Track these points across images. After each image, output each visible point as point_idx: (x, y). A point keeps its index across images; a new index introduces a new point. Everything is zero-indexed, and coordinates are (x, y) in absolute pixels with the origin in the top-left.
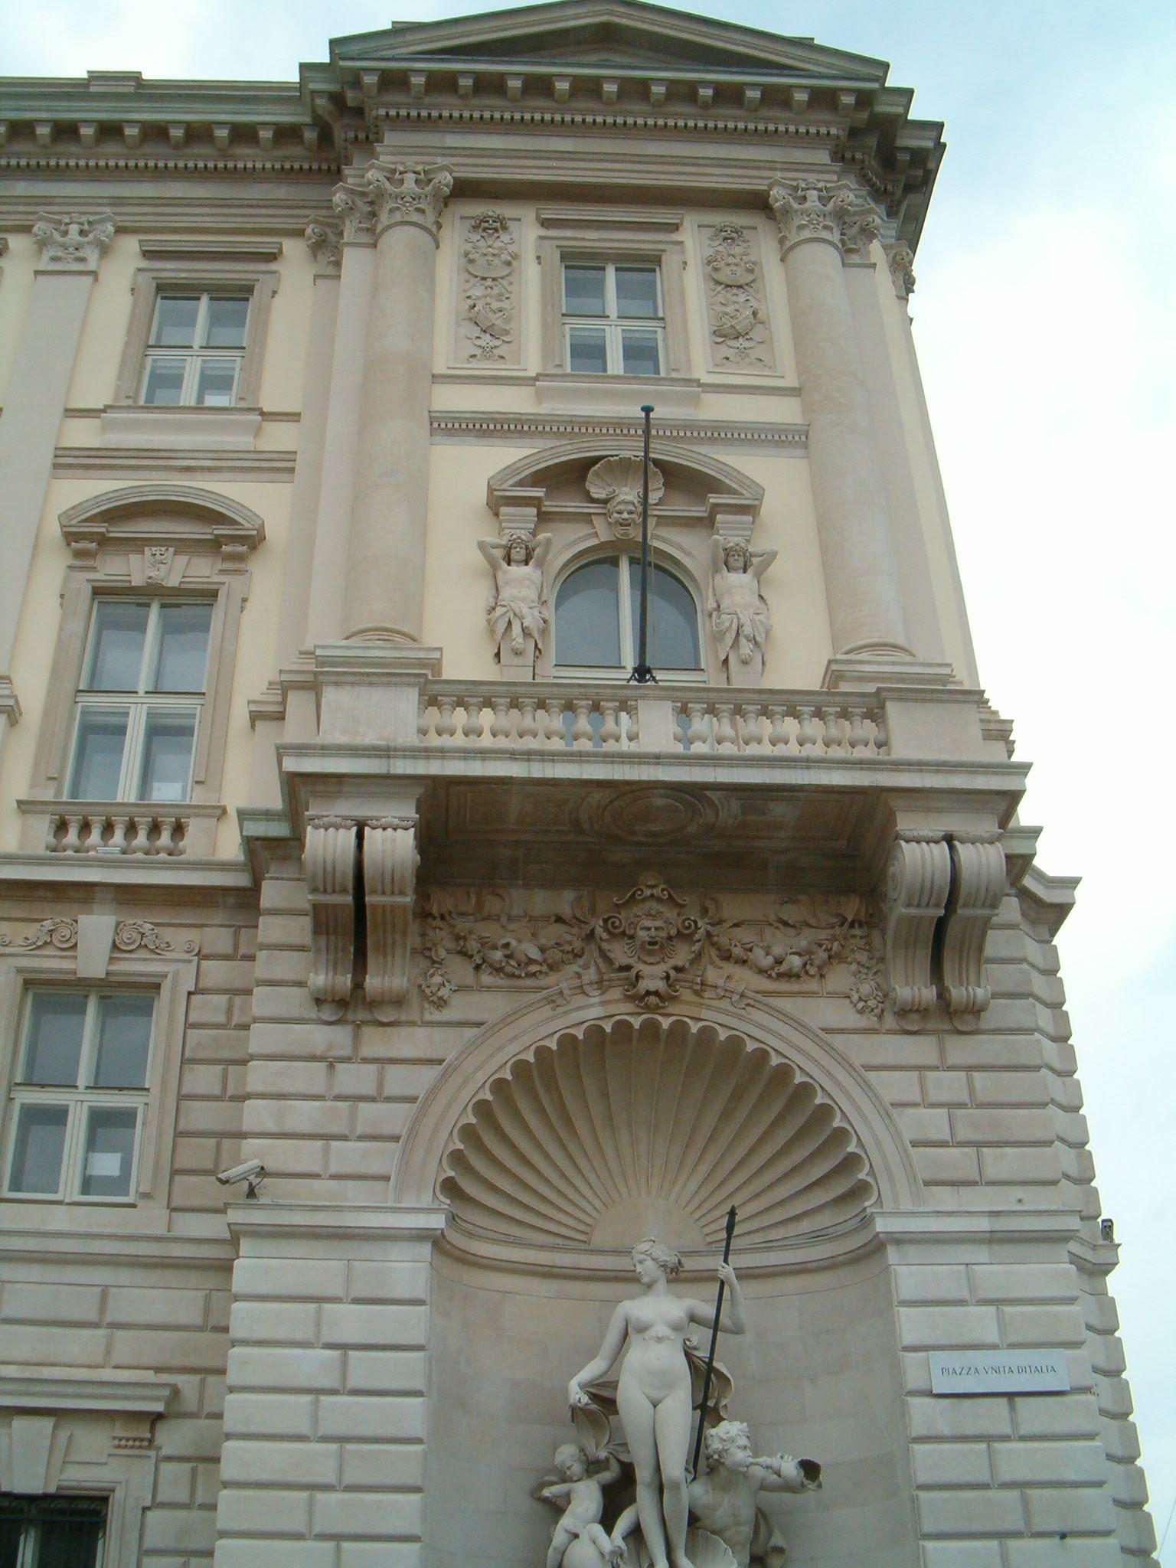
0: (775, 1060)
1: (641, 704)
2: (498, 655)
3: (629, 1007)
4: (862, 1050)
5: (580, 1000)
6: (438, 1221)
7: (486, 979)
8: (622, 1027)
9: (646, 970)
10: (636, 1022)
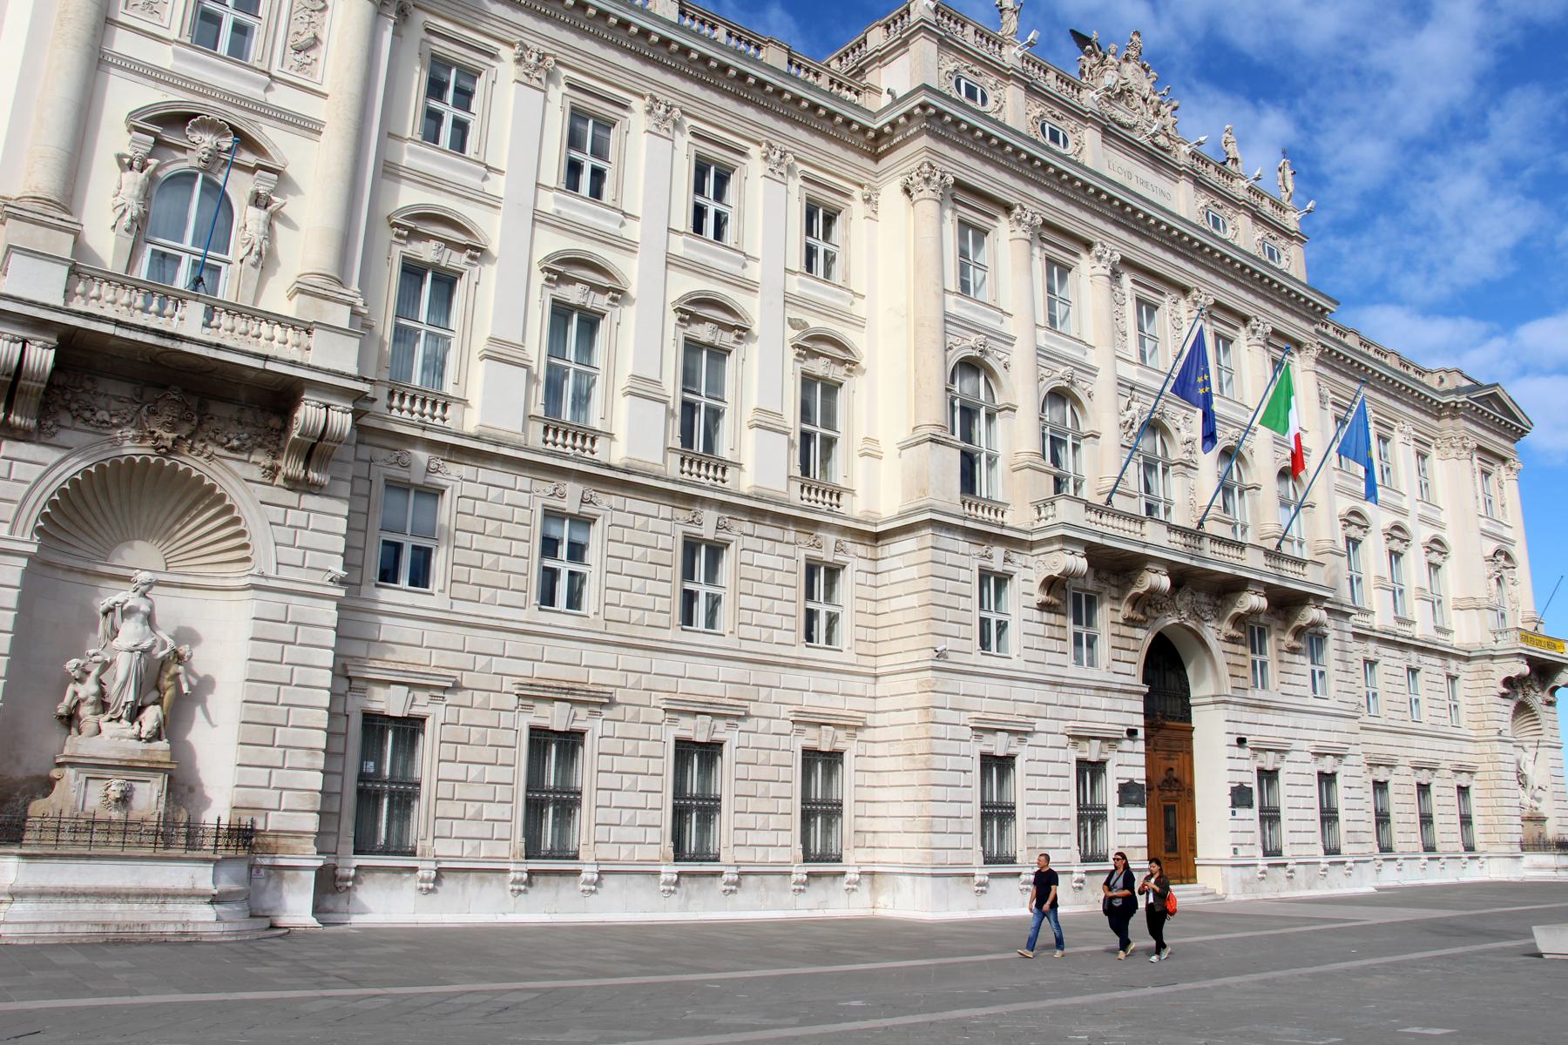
0: (218, 491)
1: (188, 302)
2: (114, 226)
3: (152, 452)
4: (264, 492)
5: (127, 443)
6: (34, 549)
7: (79, 424)
8: (145, 461)
9: (165, 435)
10: (153, 460)
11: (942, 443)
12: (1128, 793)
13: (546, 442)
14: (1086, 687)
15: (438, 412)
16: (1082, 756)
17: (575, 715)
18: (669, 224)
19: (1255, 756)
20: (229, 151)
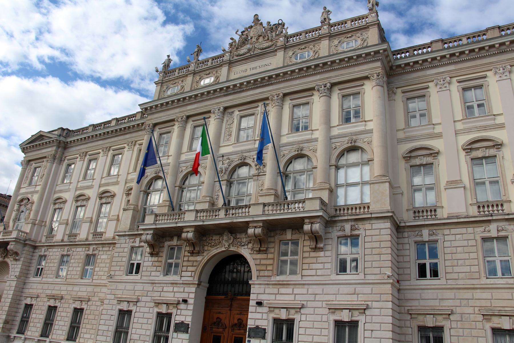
11: (127, 210)
12: (182, 327)
13: (479, 212)
14: (166, 283)
15: (500, 208)
16: (338, 318)
17: (436, 319)
18: (453, 118)
19: (157, 306)
20: (28, 202)
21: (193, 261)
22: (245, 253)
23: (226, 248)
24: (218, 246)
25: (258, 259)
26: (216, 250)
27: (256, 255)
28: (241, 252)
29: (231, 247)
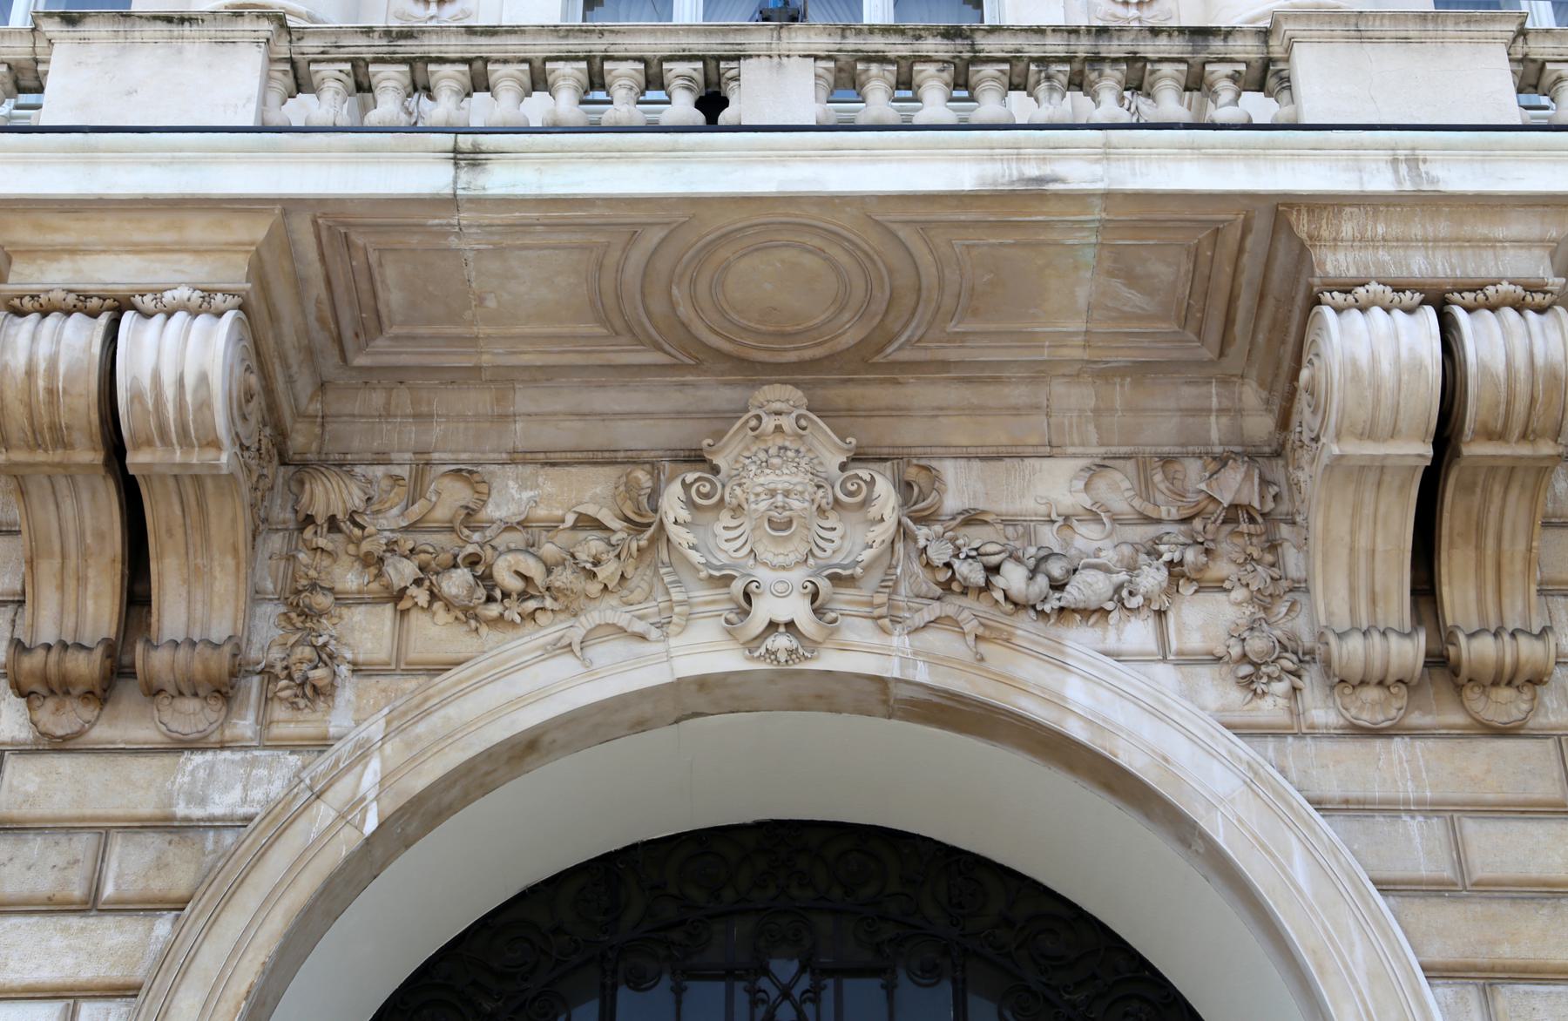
21: (104, 830)
22: (1121, 714)
23: (782, 642)
24: (608, 612)
25: (1391, 809)
26: (565, 666)
27: (1353, 749)
28: (1058, 702)
29: (858, 631)
